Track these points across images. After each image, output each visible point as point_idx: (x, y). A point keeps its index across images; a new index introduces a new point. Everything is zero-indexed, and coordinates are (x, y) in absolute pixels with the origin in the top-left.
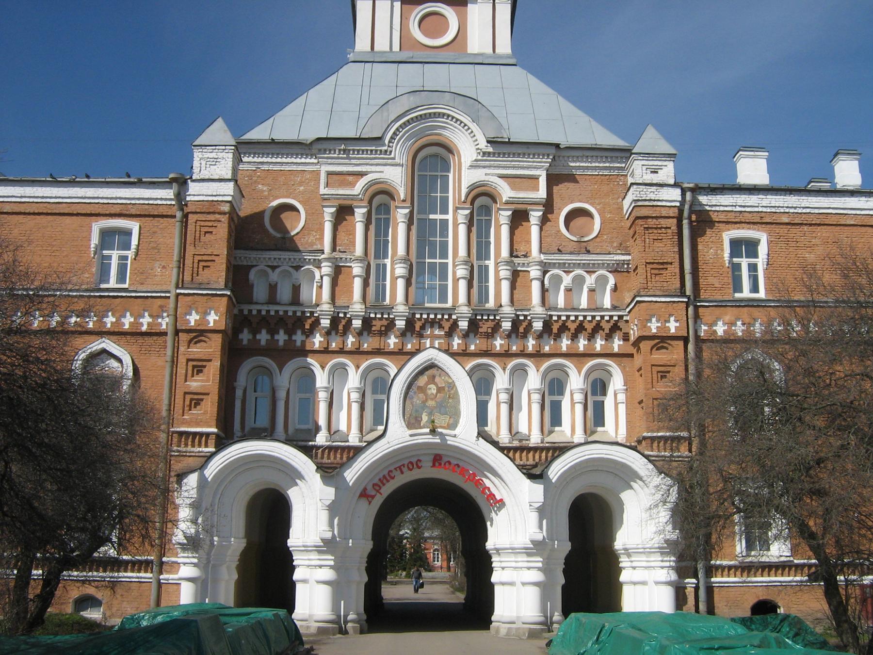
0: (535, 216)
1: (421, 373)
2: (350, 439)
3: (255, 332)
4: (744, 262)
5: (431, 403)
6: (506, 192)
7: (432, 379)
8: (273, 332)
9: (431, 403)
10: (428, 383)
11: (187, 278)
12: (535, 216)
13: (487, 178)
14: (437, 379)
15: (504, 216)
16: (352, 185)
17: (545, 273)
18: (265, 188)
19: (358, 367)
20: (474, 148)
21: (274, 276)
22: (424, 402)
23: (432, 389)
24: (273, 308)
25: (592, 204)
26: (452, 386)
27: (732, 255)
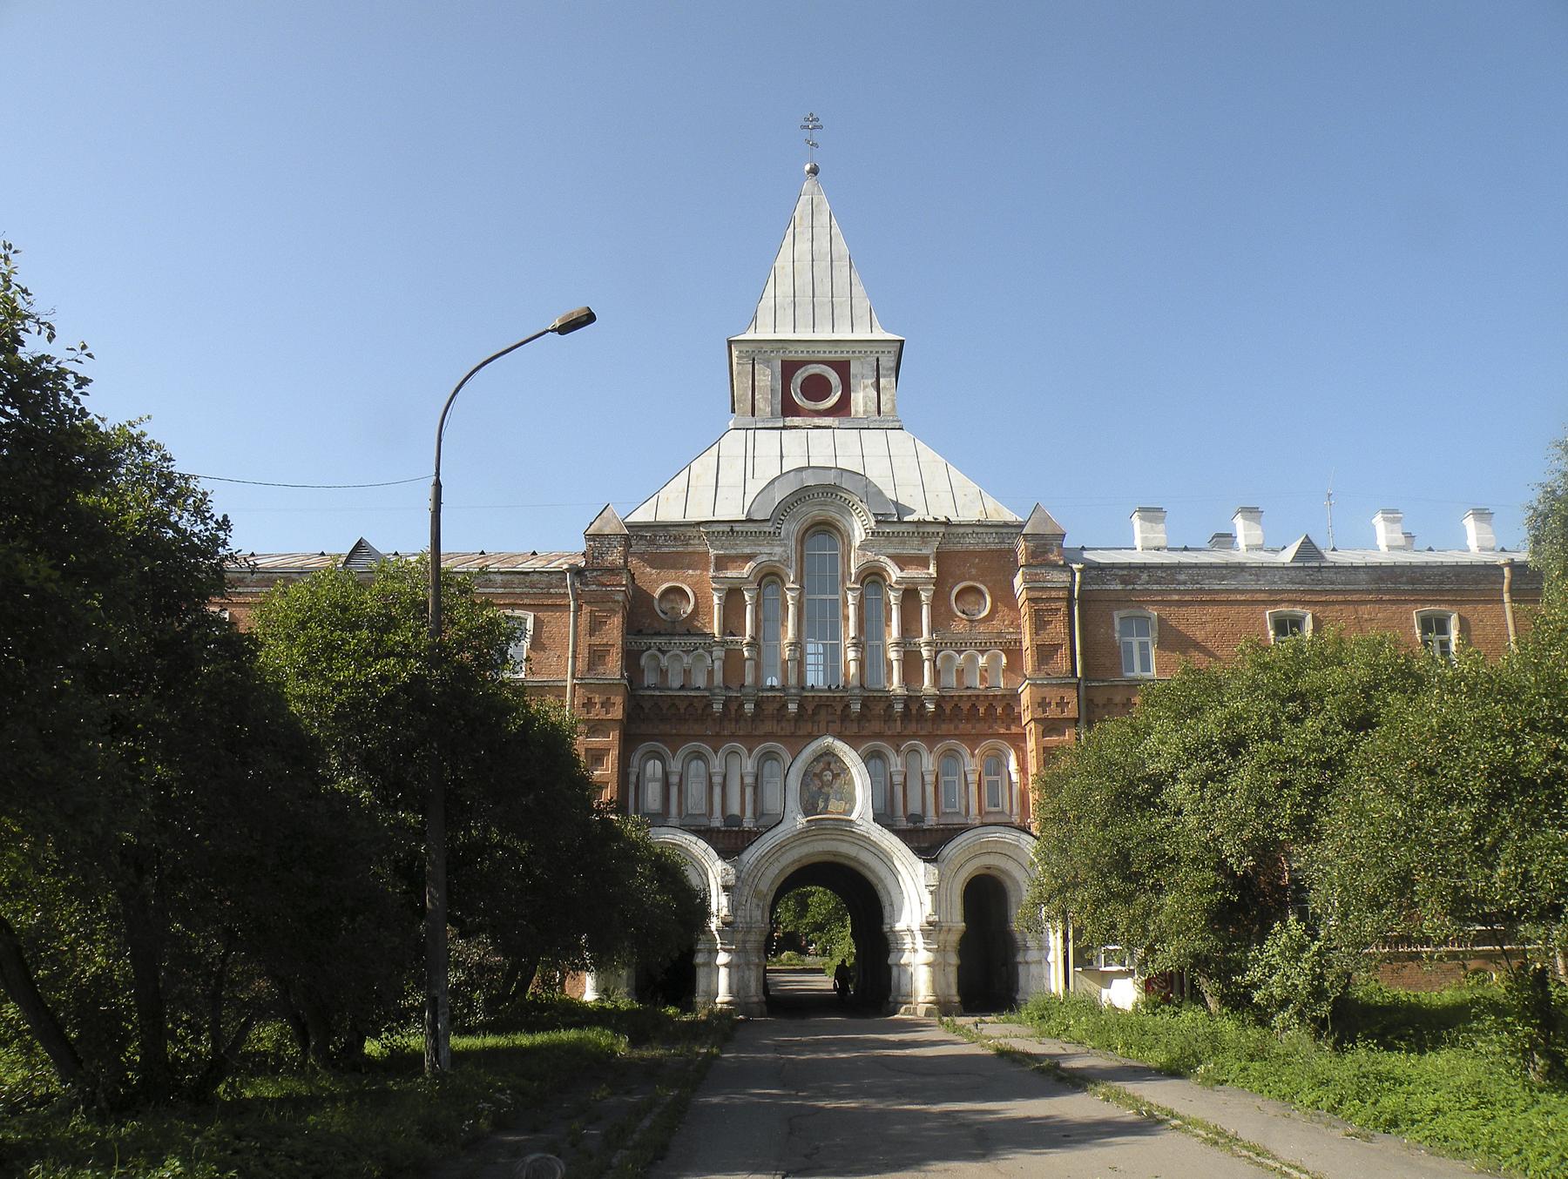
1: (817, 759)
4: (1135, 641)
6: (894, 573)
7: (828, 766)
10: (823, 770)
17: (937, 653)
19: (750, 751)
21: (664, 661)
27: (1123, 634)
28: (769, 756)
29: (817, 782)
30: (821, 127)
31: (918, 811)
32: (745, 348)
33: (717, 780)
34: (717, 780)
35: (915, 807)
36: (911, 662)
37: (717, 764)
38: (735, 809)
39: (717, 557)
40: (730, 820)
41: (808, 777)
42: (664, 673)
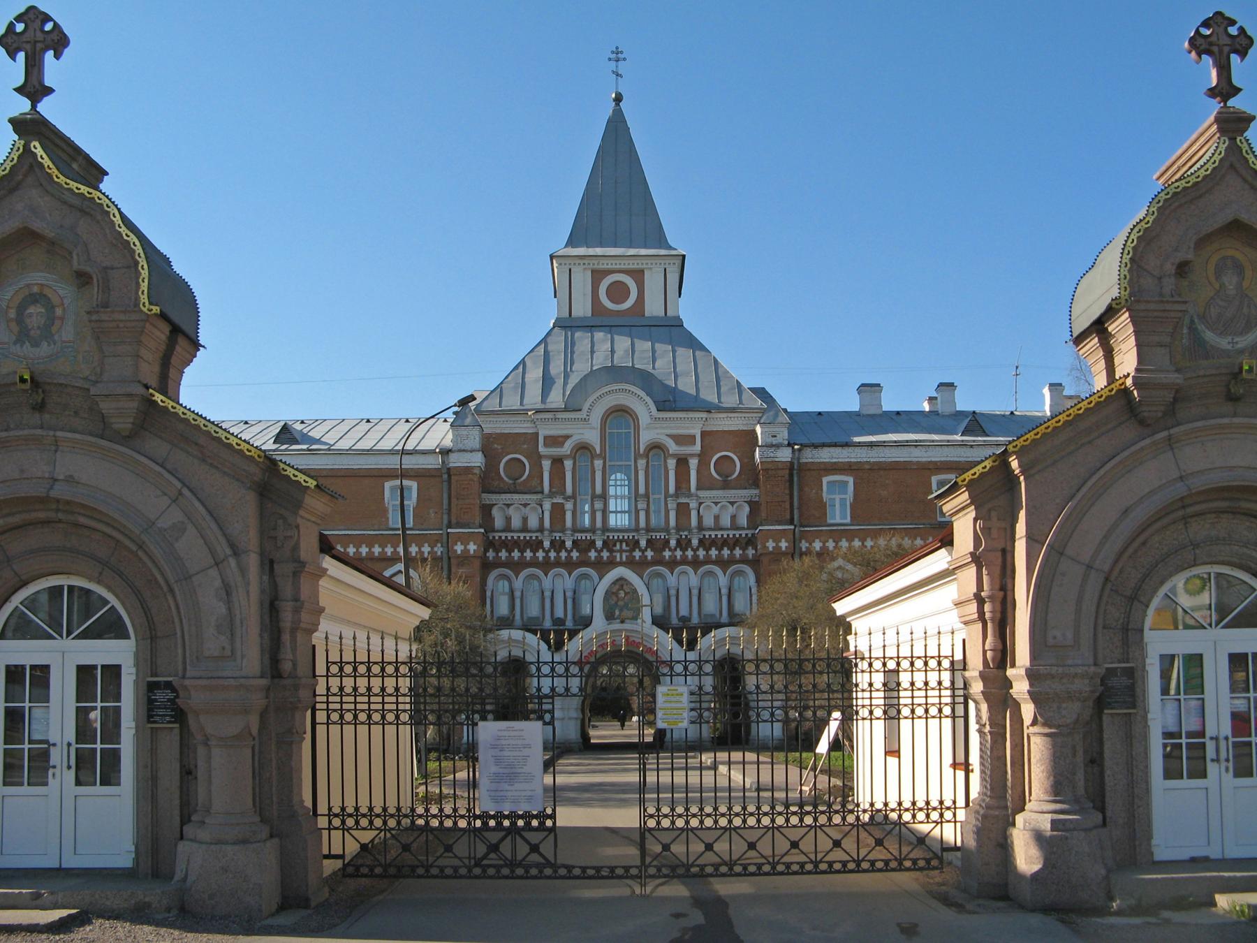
0: (693, 463)
1: (614, 583)
3: (497, 551)
4: (837, 497)
5: (621, 603)
6: (673, 447)
8: (510, 551)
9: (621, 603)
11: (454, 521)
12: (693, 463)
15: (672, 463)
16: (562, 444)
17: (700, 504)
21: (511, 511)
23: (622, 594)
24: (509, 535)
26: (635, 591)
27: (829, 492)
28: (585, 576)
32: (563, 261)
33: (547, 594)
34: (547, 594)
35: (684, 612)
36: (683, 510)
37: (547, 582)
38: (559, 613)
40: (559, 622)
41: (608, 595)
42: (508, 519)
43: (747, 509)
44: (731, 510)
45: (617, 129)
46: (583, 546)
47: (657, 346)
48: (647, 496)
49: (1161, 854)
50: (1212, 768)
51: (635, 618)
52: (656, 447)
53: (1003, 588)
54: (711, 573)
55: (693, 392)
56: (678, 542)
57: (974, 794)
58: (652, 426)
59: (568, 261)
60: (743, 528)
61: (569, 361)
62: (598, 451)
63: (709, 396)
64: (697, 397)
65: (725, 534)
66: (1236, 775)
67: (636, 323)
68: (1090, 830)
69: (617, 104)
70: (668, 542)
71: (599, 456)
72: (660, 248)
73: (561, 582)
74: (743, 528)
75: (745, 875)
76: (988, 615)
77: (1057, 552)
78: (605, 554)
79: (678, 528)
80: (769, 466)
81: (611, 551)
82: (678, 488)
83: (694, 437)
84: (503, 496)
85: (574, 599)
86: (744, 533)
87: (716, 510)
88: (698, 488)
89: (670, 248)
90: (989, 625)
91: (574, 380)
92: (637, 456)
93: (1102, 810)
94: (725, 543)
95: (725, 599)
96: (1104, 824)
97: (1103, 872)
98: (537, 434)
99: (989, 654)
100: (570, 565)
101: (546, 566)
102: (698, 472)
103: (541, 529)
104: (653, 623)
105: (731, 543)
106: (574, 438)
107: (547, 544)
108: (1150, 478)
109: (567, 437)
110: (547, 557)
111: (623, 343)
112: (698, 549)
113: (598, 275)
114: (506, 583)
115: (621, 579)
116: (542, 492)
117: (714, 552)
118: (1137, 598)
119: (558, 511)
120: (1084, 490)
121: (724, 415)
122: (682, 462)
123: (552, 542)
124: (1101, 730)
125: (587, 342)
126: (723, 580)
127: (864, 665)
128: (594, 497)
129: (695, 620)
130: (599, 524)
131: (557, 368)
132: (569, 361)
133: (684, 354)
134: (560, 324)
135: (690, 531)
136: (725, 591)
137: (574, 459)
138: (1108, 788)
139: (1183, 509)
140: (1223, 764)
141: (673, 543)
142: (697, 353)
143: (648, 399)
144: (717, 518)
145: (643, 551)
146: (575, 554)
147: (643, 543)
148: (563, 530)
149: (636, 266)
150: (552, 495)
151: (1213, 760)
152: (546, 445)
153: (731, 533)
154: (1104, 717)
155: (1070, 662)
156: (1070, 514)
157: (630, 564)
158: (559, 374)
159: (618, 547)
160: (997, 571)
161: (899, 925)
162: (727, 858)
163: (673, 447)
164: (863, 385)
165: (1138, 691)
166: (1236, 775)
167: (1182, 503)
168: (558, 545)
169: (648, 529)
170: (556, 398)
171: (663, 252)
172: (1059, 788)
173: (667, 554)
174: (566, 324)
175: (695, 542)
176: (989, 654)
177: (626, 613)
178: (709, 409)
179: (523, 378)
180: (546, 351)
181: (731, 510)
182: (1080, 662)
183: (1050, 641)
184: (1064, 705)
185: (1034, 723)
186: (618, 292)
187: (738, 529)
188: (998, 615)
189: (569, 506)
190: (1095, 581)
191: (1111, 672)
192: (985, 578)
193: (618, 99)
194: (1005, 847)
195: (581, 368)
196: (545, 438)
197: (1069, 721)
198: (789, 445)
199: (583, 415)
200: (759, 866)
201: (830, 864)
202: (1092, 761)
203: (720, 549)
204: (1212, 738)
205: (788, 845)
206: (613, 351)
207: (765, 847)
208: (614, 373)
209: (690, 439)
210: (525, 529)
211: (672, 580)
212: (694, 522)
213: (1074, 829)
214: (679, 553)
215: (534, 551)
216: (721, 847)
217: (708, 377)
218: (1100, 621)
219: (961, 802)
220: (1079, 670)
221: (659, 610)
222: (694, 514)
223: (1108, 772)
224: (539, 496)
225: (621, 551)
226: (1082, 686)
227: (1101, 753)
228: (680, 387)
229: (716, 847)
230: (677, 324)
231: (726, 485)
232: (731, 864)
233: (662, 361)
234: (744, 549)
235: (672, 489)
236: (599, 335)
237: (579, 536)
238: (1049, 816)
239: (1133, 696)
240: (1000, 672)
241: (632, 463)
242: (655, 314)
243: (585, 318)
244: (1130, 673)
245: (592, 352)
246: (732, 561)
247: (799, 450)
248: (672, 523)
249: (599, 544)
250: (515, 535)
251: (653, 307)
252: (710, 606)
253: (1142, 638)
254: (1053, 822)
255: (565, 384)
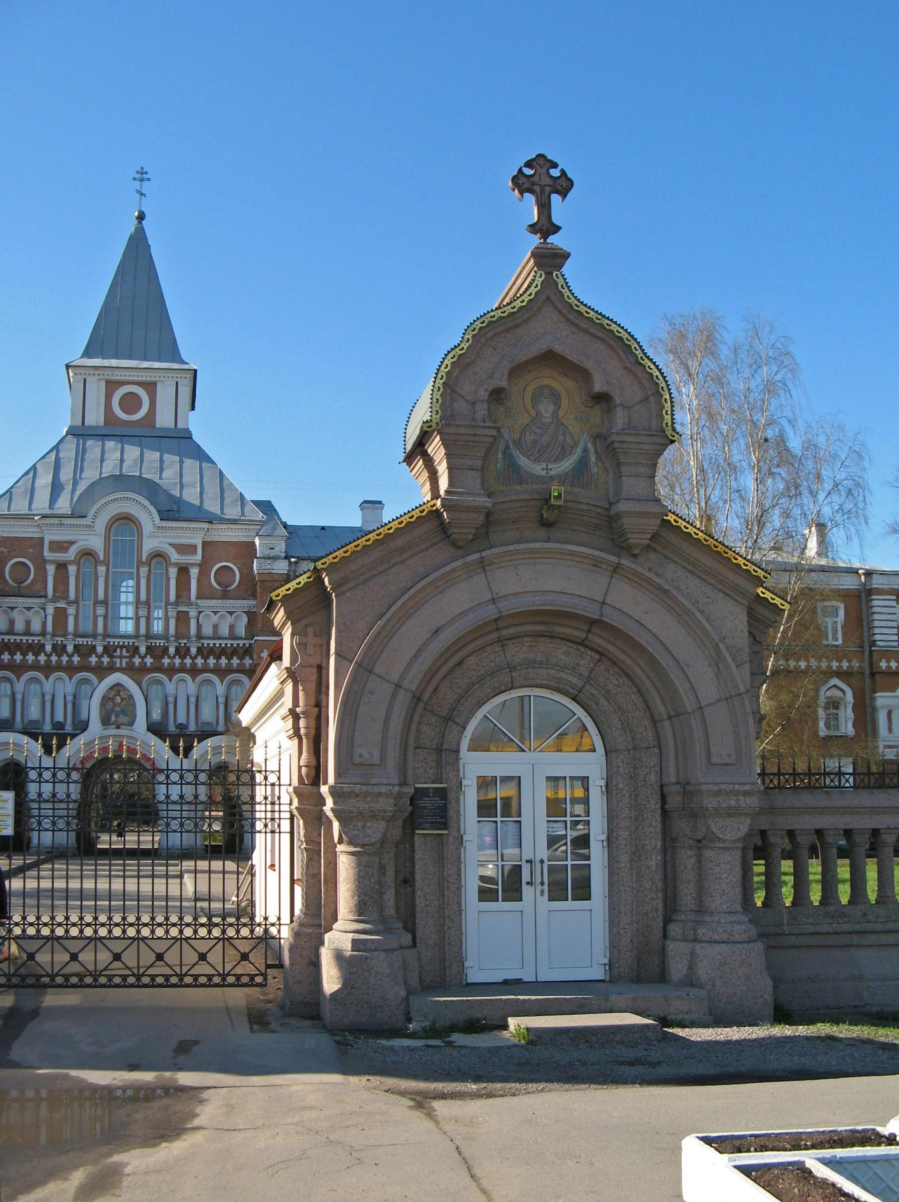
0: (194, 572)
1: (111, 688)
2: (66, 728)
5: (117, 709)
6: (174, 556)
7: (118, 694)
9: (117, 709)
12: (194, 572)
13: (160, 545)
14: (121, 693)
15: (173, 572)
17: (200, 612)
18: (5, 550)
19: (70, 678)
20: (151, 524)
21: (15, 614)
22: (113, 708)
25: (234, 564)
26: (131, 697)
28: (86, 681)
29: (111, 704)
30: (149, 180)
31: (184, 722)
32: (78, 371)
33: (48, 698)
34: (48, 698)
35: (182, 719)
36: (183, 618)
37: (48, 686)
38: (59, 717)
39: (51, 543)
41: (105, 699)
43: (245, 619)
44: (230, 619)
45: (138, 245)
46: (85, 651)
47: (166, 457)
48: (148, 603)
49: (474, 976)
50: (527, 891)
51: (131, 723)
52: (158, 555)
53: (318, 705)
54: (208, 681)
55: (197, 502)
56: (177, 649)
57: (297, 912)
58: (155, 535)
59: (83, 371)
60: (241, 638)
61: (79, 468)
62: (102, 558)
63: (212, 506)
64: (200, 508)
65: (223, 642)
66: (551, 899)
67: (147, 434)
68: (393, 950)
69: (140, 223)
70: (166, 649)
71: (102, 563)
72: (173, 361)
73: (62, 686)
74: (241, 638)
75: (81, 986)
76: (302, 731)
77: (365, 670)
78: (106, 660)
79: (178, 636)
80: (267, 578)
81: (111, 657)
82: (178, 596)
83: (195, 546)
84: (8, 599)
85: (74, 704)
86: (241, 642)
87: (215, 619)
88: (198, 597)
89: (184, 362)
90: (304, 741)
91: (82, 487)
92: (140, 563)
93: (413, 932)
94: (223, 652)
95: (222, 708)
96: (414, 945)
97: (403, 993)
98: (42, 539)
99: (304, 770)
100: (71, 670)
101: (48, 669)
102: (199, 581)
103: (43, 633)
104: (149, 729)
105: (229, 652)
106: (78, 545)
107: (48, 648)
108: (462, 600)
109: (72, 543)
110: (48, 661)
111: (132, 452)
112: (196, 657)
113: (112, 386)
114: (8, 685)
115: (118, 685)
116: (46, 596)
117: (212, 661)
118: (453, 719)
119: (61, 615)
120: (394, 609)
121: (225, 526)
122: (183, 571)
123: (54, 646)
124: (413, 851)
125: (98, 450)
126: (221, 689)
127: (161, 778)
128: (96, 602)
129: (192, 728)
130: (100, 629)
131: (66, 474)
132: (79, 468)
133: (191, 464)
134: (73, 432)
135: (189, 638)
136: (221, 700)
137: (78, 564)
138: (418, 909)
139: (499, 629)
140: (539, 888)
141: (172, 650)
142: (204, 465)
143: (152, 509)
144: (215, 627)
145: (143, 658)
146: (76, 659)
147: (143, 650)
148: (65, 635)
149: (149, 379)
150: (55, 599)
151: (528, 883)
152: (50, 550)
153: (229, 642)
154: (416, 837)
155: (374, 781)
156: (379, 633)
157: (130, 670)
158: (69, 481)
159: (118, 653)
160: (313, 686)
161: (196, 1042)
162: (91, 968)
163: (174, 556)
164: (366, 502)
165: (451, 812)
166: (551, 899)
167: (497, 622)
168: (59, 649)
169: (148, 636)
170: (64, 505)
171: (175, 366)
172: (364, 907)
173: (166, 661)
174: (80, 432)
175: (194, 650)
176: (304, 770)
177: (123, 719)
178: (211, 519)
179: (33, 483)
180: (57, 459)
181: (230, 619)
182: (385, 781)
183: (357, 760)
184: (369, 824)
185: (341, 841)
186: (130, 403)
187: (235, 638)
188: (313, 731)
189: (71, 611)
190: (403, 700)
191: (419, 793)
192: (301, 693)
193: (141, 217)
194: (316, 965)
195: (91, 475)
196: (51, 543)
197: (373, 840)
198: (286, 558)
199: (87, 521)
200: (124, 978)
201: (196, 977)
202: (405, 882)
203: (218, 658)
204: (527, 861)
205: (153, 957)
206: (122, 460)
207: (129, 958)
208: (121, 481)
209: (192, 549)
210: (27, 632)
211: (170, 687)
212: (193, 630)
213: (375, 950)
214: (177, 661)
215: (36, 654)
216: (86, 957)
217: (212, 489)
218: (411, 741)
219: (286, 919)
220: (383, 789)
221: (156, 715)
222: (193, 623)
223: (419, 893)
224: (43, 600)
225: (121, 657)
226: (386, 805)
227: (412, 873)
228: (186, 496)
229: (81, 957)
230: (186, 436)
231: (225, 595)
232: (96, 976)
233: (168, 471)
234: (242, 658)
235: (172, 598)
236: (110, 444)
237: (80, 641)
238: (351, 936)
239: (445, 817)
240: (315, 788)
241: (135, 570)
242: (165, 426)
243: (98, 427)
244: (442, 793)
245: (102, 460)
246: (229, 670)
247: (296, 563)
248: (172, 630)
249: (100, 649)
250: (18, 638)
251: (164, 419)
252: (207, 713)
253: (457, 759)
254: (354, 941)
255: (73, 491)
